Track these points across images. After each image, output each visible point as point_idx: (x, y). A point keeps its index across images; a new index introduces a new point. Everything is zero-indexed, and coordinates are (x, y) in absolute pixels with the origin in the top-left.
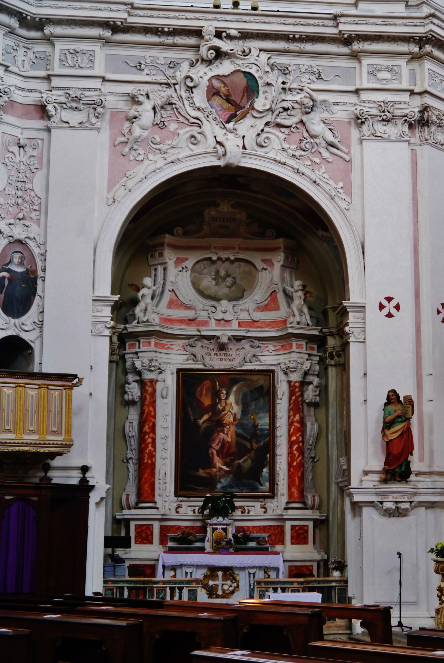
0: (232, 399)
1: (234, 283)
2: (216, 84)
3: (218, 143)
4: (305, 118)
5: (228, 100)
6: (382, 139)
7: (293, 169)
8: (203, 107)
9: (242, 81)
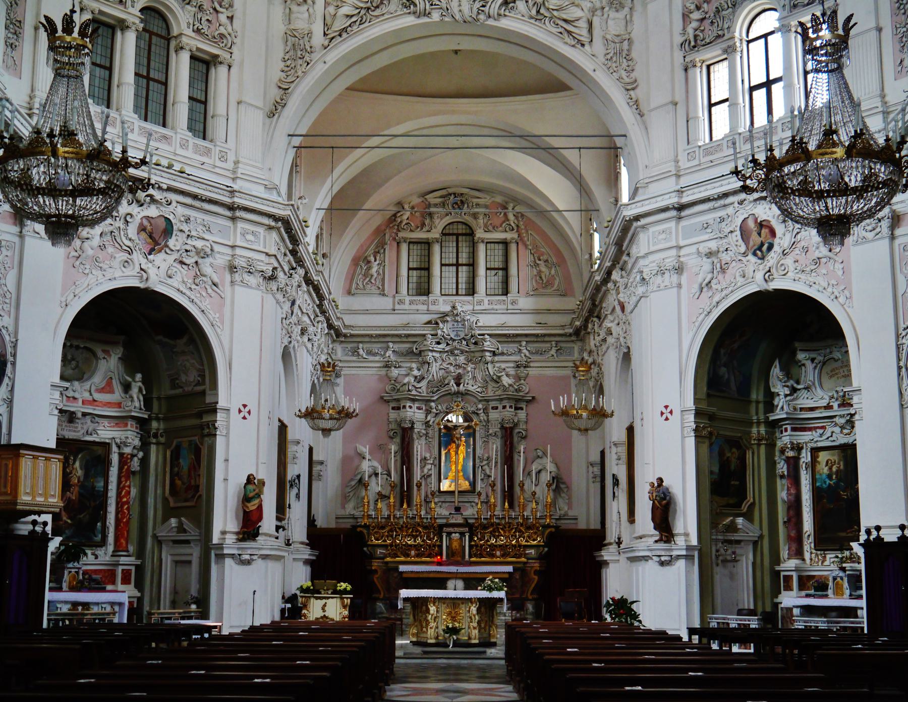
0: (77, 464)
1: (77, 366)
2: (145, 223)
3: (142, 269)
4: (200, 261)
5: (151, 237)
6: (247, 286)
8: (133, 238)
9: (162, 224)
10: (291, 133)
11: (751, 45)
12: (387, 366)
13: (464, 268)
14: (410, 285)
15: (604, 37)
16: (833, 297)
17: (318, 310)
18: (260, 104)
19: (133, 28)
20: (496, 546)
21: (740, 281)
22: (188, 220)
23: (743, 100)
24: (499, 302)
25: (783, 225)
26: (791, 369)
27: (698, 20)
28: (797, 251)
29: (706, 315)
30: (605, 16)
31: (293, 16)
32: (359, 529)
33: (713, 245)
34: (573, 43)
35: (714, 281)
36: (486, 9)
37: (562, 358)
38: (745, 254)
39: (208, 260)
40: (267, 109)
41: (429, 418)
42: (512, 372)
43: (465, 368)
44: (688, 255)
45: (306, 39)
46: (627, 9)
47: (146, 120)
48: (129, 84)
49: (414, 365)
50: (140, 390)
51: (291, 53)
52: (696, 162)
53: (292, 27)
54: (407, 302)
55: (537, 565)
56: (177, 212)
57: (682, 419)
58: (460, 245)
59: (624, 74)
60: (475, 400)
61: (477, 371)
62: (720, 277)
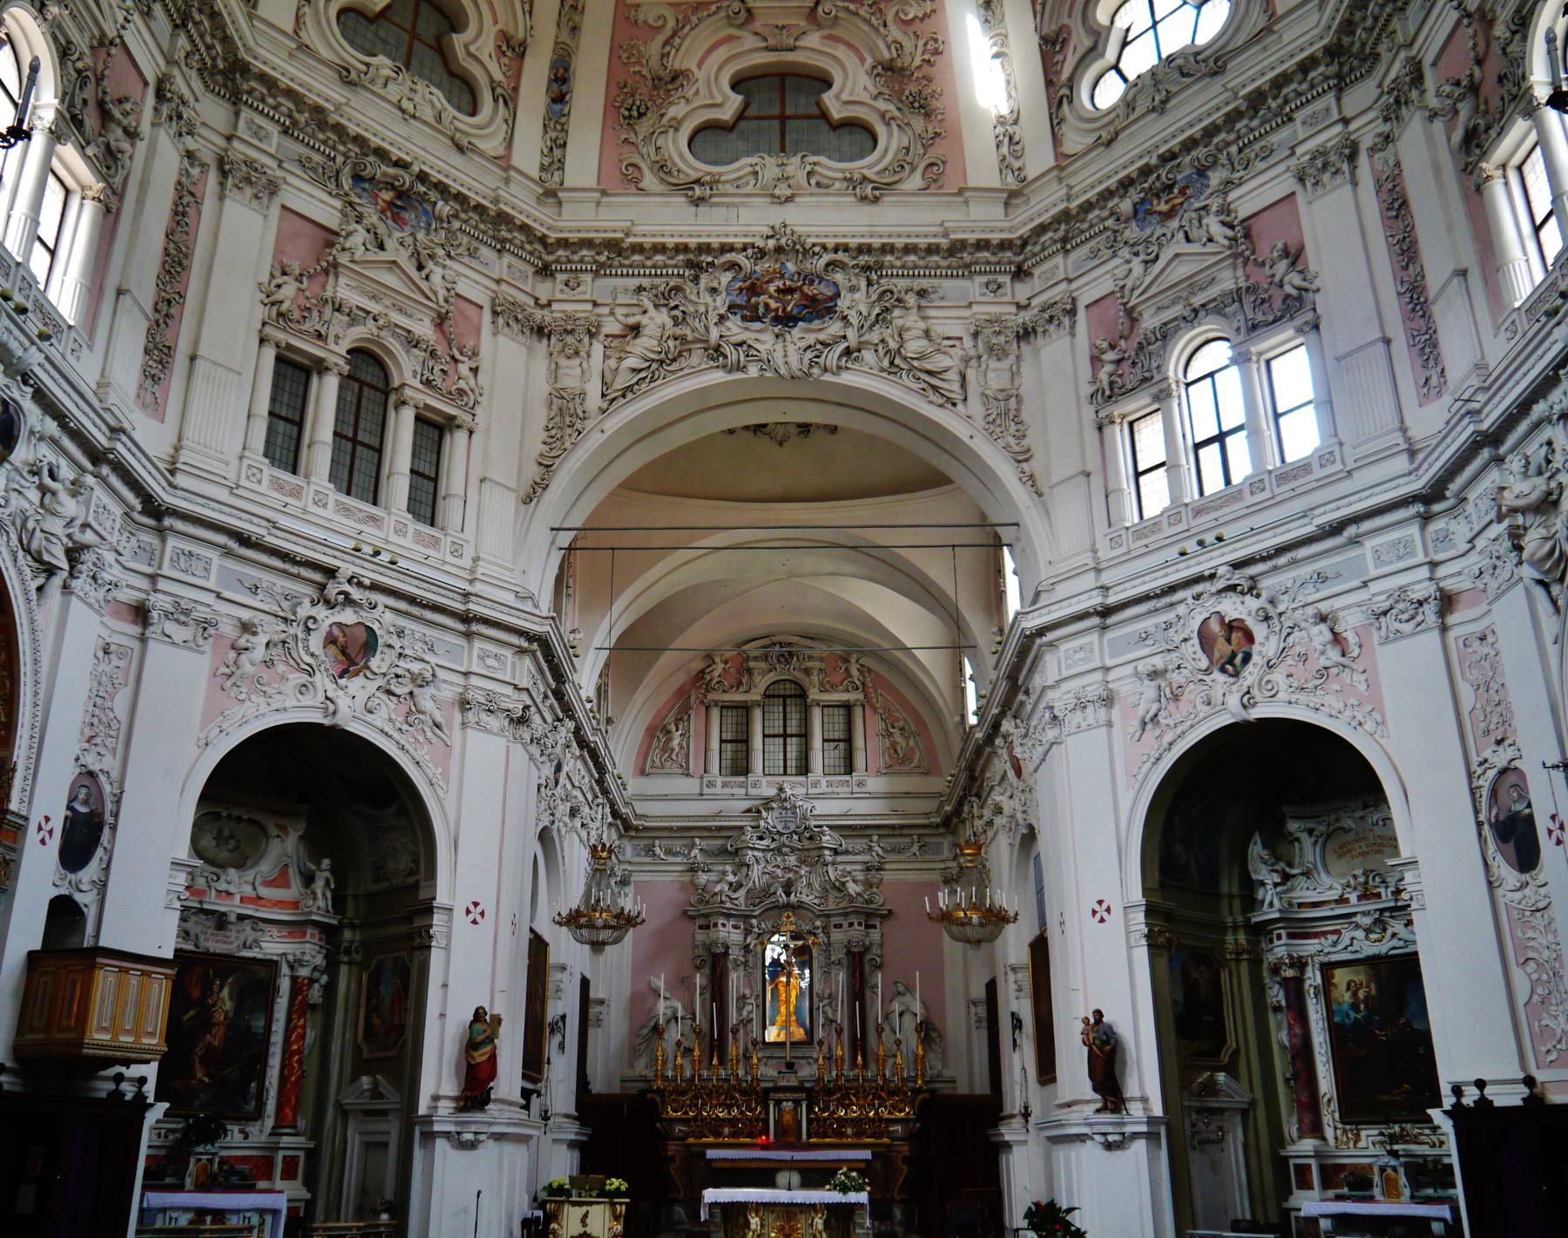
2: (336, 632)
3: (327, 698)
4: (417, 691)
5: (344, 653)
6: (486, 730)
7: (398, 743)
8: (317, 653)
9: (362, 635)
11: (1191, 389)
12: (693, 869)
13: (794, 739)
14: (724, 762)
15: (983, 394)
16: (1354, 723)
17: (597, 789)
18: (513, 484)
19: (335, 371)
20: (846, 1120)
21: (1203, 710)
22: (400, 633)
23: (1186, 461)
24: (841, 783)
25: (1265, 625)
26: (1280, 846)
27: (1112, 362)
28: (1289, 661)
29: (1154, 764)
30: (984, 366)
31: (560, 372)
32: (649, 1096)
33: (1158, 662)
34: (941, 401)
35: (1163, 713)
36: (821, 361)
37: (928, 857)
38: (1207, 671)
39: (430, 690)
40: (522, 493)
41: (749, 940)
42: (860, 876)
43: (796, 872)
44: (1119, 679)
45: (578, 401)
46: (1012, 358)
47: (348, 493)
48: (324, 443)
49: (728, 868)
50: (327, 883)
51: (558, 419)
52: (1124, 549)
53: (559, 386)
54: (719, 784)
55: (906, 1148)
56: (383, 619)
57: (1126, 920)
58: (788, 710)
59: (1012, 441)
60: (810, 914)
61: (813, 876)
62: (1172, 706)
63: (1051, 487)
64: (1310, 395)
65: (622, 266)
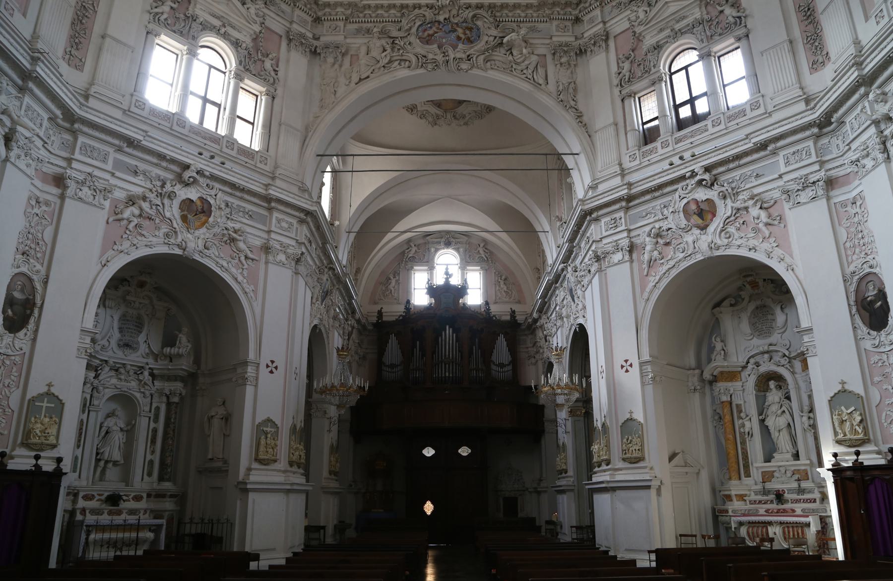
10: (321, 153)
56: (218, 198)
57: (641, 370)
63: (596, 132)
64: (744, 74)
65: (359, 17)
